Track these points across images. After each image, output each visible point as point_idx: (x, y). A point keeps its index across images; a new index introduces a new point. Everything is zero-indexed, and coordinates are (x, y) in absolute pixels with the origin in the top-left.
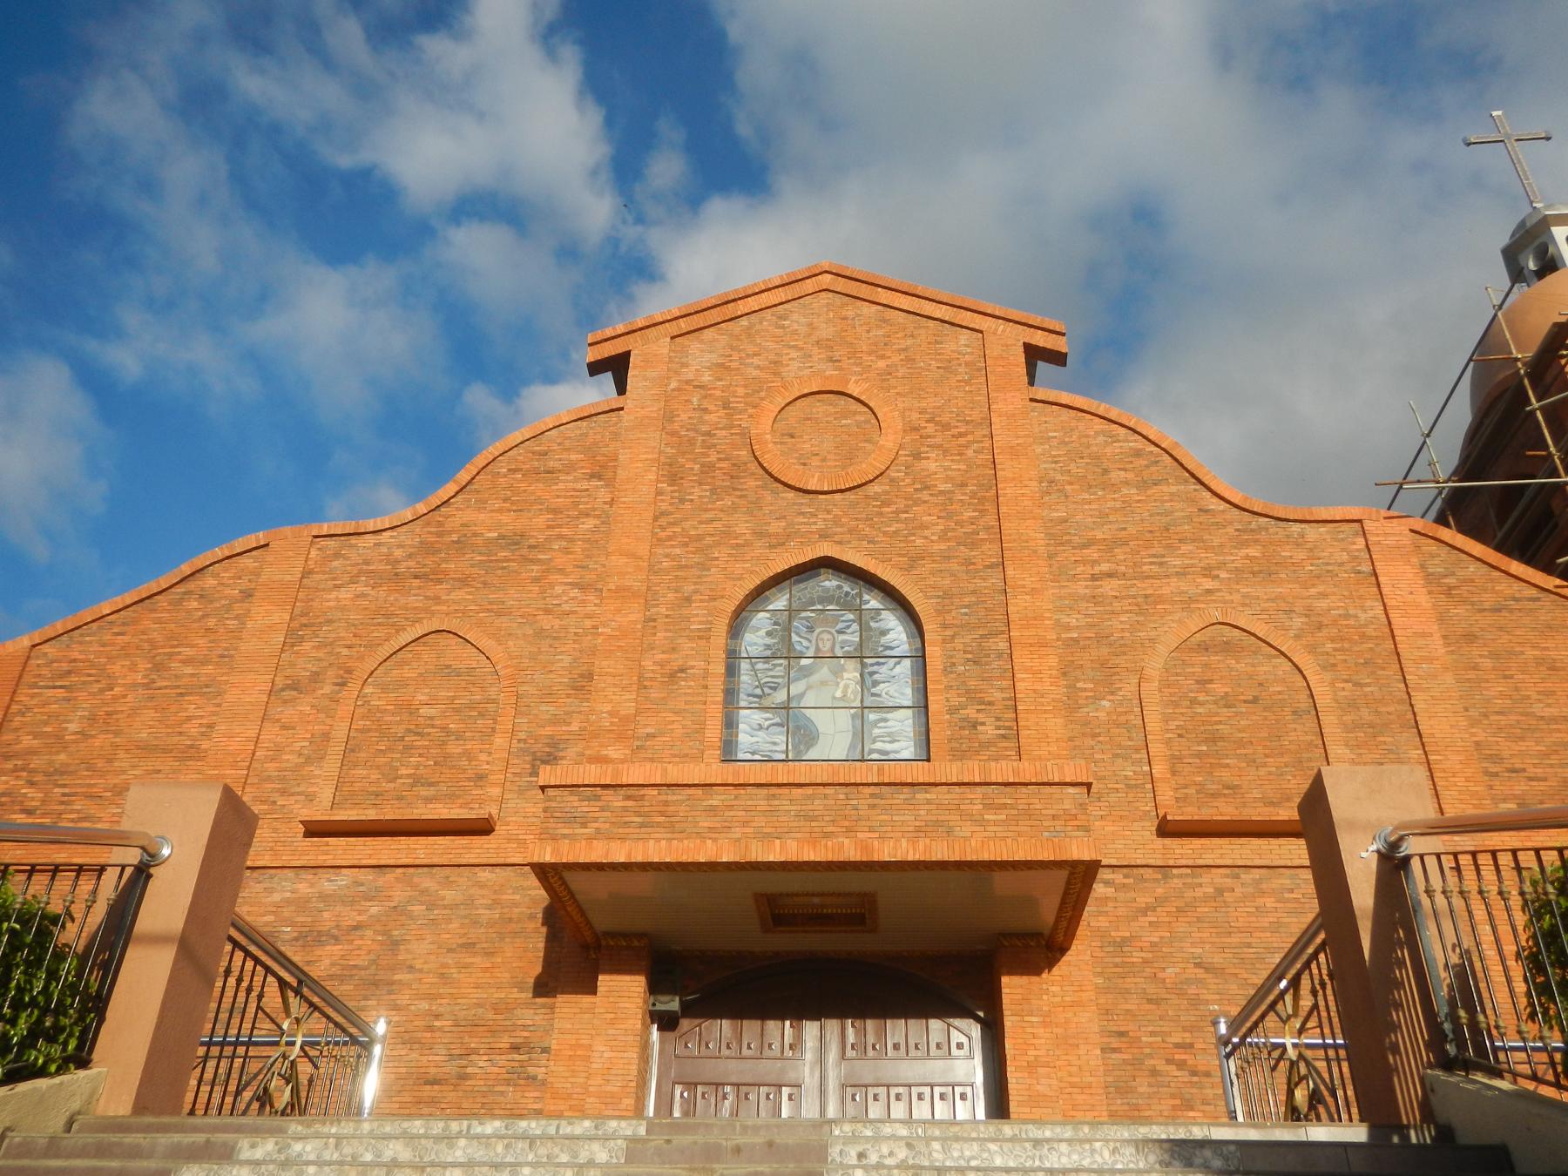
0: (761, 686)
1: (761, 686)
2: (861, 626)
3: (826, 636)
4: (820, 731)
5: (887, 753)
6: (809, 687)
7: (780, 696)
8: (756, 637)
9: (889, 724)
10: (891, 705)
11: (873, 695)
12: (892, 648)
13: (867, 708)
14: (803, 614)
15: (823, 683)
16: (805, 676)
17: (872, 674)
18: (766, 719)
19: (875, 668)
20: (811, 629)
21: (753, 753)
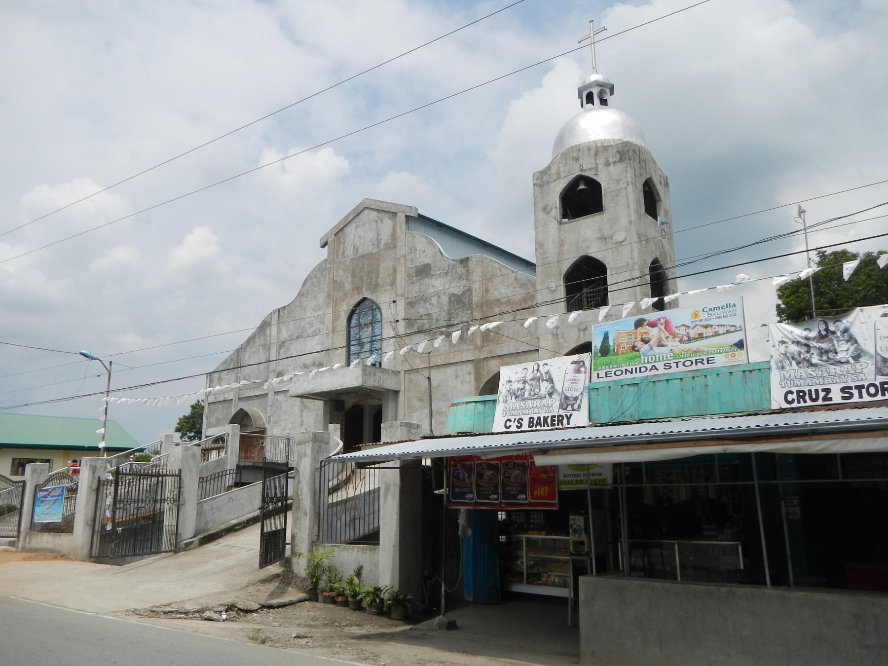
6: (363, 333)
7: (358, 336)
12: (377, 319)
15: (365, 331)
20: (363, 317)
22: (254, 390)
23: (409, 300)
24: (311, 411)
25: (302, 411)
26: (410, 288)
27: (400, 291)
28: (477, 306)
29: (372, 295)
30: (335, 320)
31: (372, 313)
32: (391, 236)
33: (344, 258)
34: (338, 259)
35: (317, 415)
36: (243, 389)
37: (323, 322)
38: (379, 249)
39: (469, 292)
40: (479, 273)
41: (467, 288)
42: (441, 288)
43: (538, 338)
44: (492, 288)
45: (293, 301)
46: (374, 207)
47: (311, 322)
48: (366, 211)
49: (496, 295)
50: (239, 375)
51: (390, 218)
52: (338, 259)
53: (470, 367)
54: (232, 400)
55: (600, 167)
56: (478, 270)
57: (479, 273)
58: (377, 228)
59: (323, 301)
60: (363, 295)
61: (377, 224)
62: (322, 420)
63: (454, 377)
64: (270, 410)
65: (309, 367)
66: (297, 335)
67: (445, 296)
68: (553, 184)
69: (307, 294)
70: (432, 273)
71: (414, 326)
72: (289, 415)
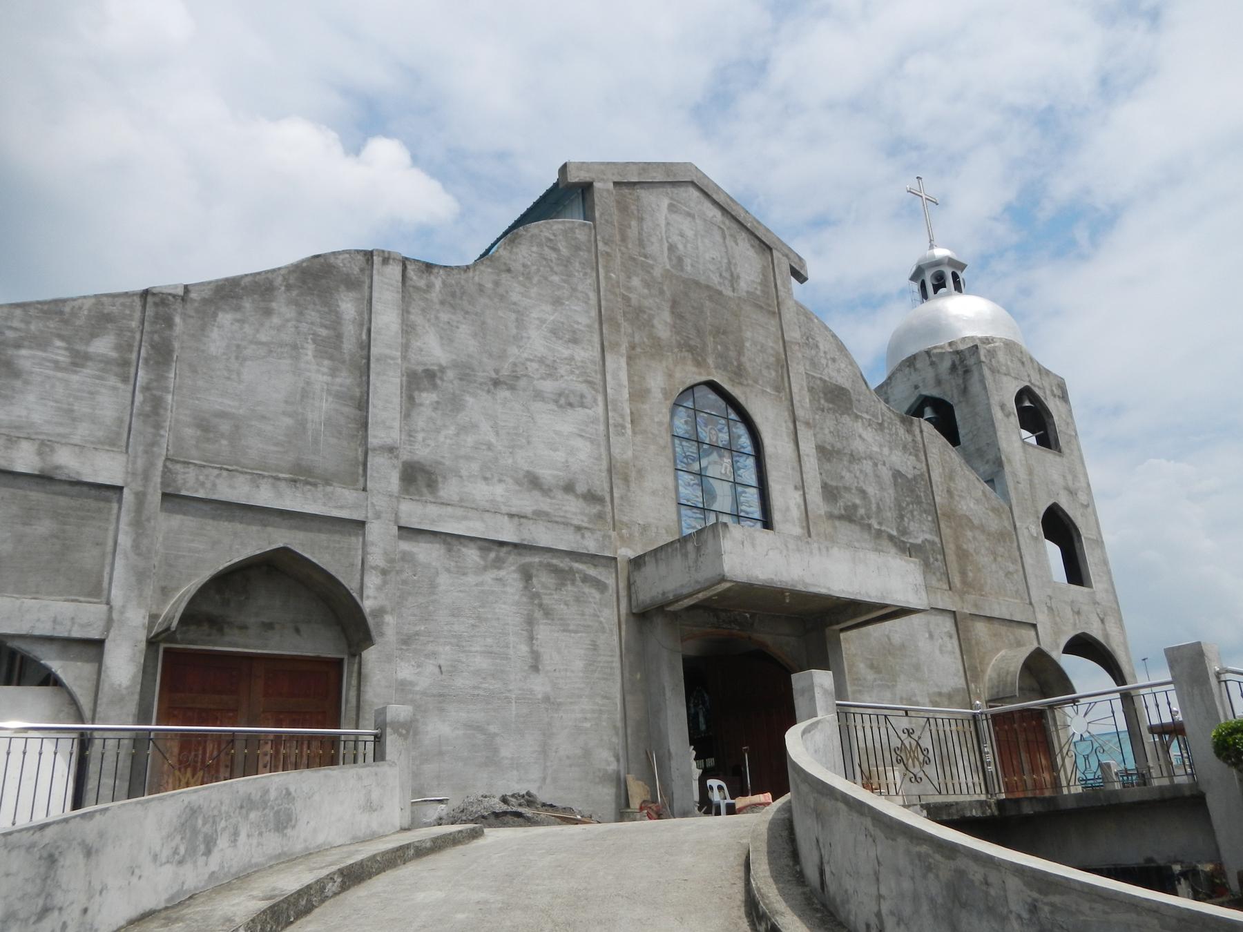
1: (686, 457)
2: (729, 428)
3: (713, 432)
5: (747, 513)
6: (709, 463)
7: (696, 467)
11: (739, 476)
12: (744, 448)
14: (702, 414)
15: (715, 463)
16: (708, 455)
17: (737, 462)
18: (692, 480)
19: (737, 458)
20: (706, 426)
21: (688, 501)
22: (274, 486)
23: (820, 444)
24: (564, 631)
25: (530, 622)
26: (817, 417)
27: (800, 413)
28: (944, 515)
29: (733, 385)
30: (639, 394)
32: (760, 284)
33: (646, 257)
34: (627, 248)
35: (595, 647)
36: (204, 466)
37: (595, 384)
38: (735, 295)
39: (923, 480)
40: (936, 456)
41: (919, 473)
42: (876, 449)
43: (1031, 604)
44: (955, 492)
45: (468, 267)
46: (715, 196)
47: (548, 362)
48: (695, 194)
49: (965, 508)
50: (169, 397)
51: (753, 246)
52: (627, 248)
53: (947, 624)
54: (121, 489)
55: (1048, 392)
56: (934, 451)
57: (936, 456)
58: (726, 247)
59: (588, 326)
60: (709, 374)
61: (724, 238)
62: (617, 664)
63: (927, 635)
64: (379, 588)
65: (550, 490)
66: (494, 375)
67: (884, 468)
68: (1005, 379)
69: (528, 277)
70: (855, 411)
71: (837, 501)
72: (473, 626)
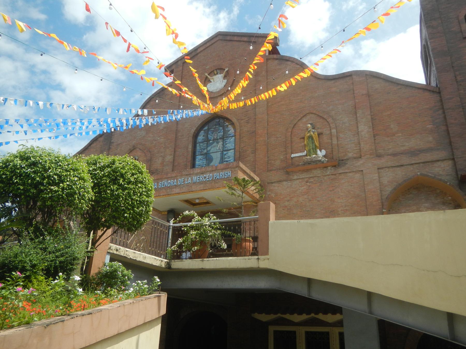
0: (201, 149)
3: (215, 134)
4: (214, 158)
7: (205, 151)
8: (201, 138)
9: (229, 154)
10: (229, 149)
11: (226, 147)
12: (230, 135)
13: (224, 150)
14: (211, 130)
15: (215, 146)
16: (211, 145)
18: (202, 157)
19: (226, 140)
20: (213, 133)
31: (224, 129)
